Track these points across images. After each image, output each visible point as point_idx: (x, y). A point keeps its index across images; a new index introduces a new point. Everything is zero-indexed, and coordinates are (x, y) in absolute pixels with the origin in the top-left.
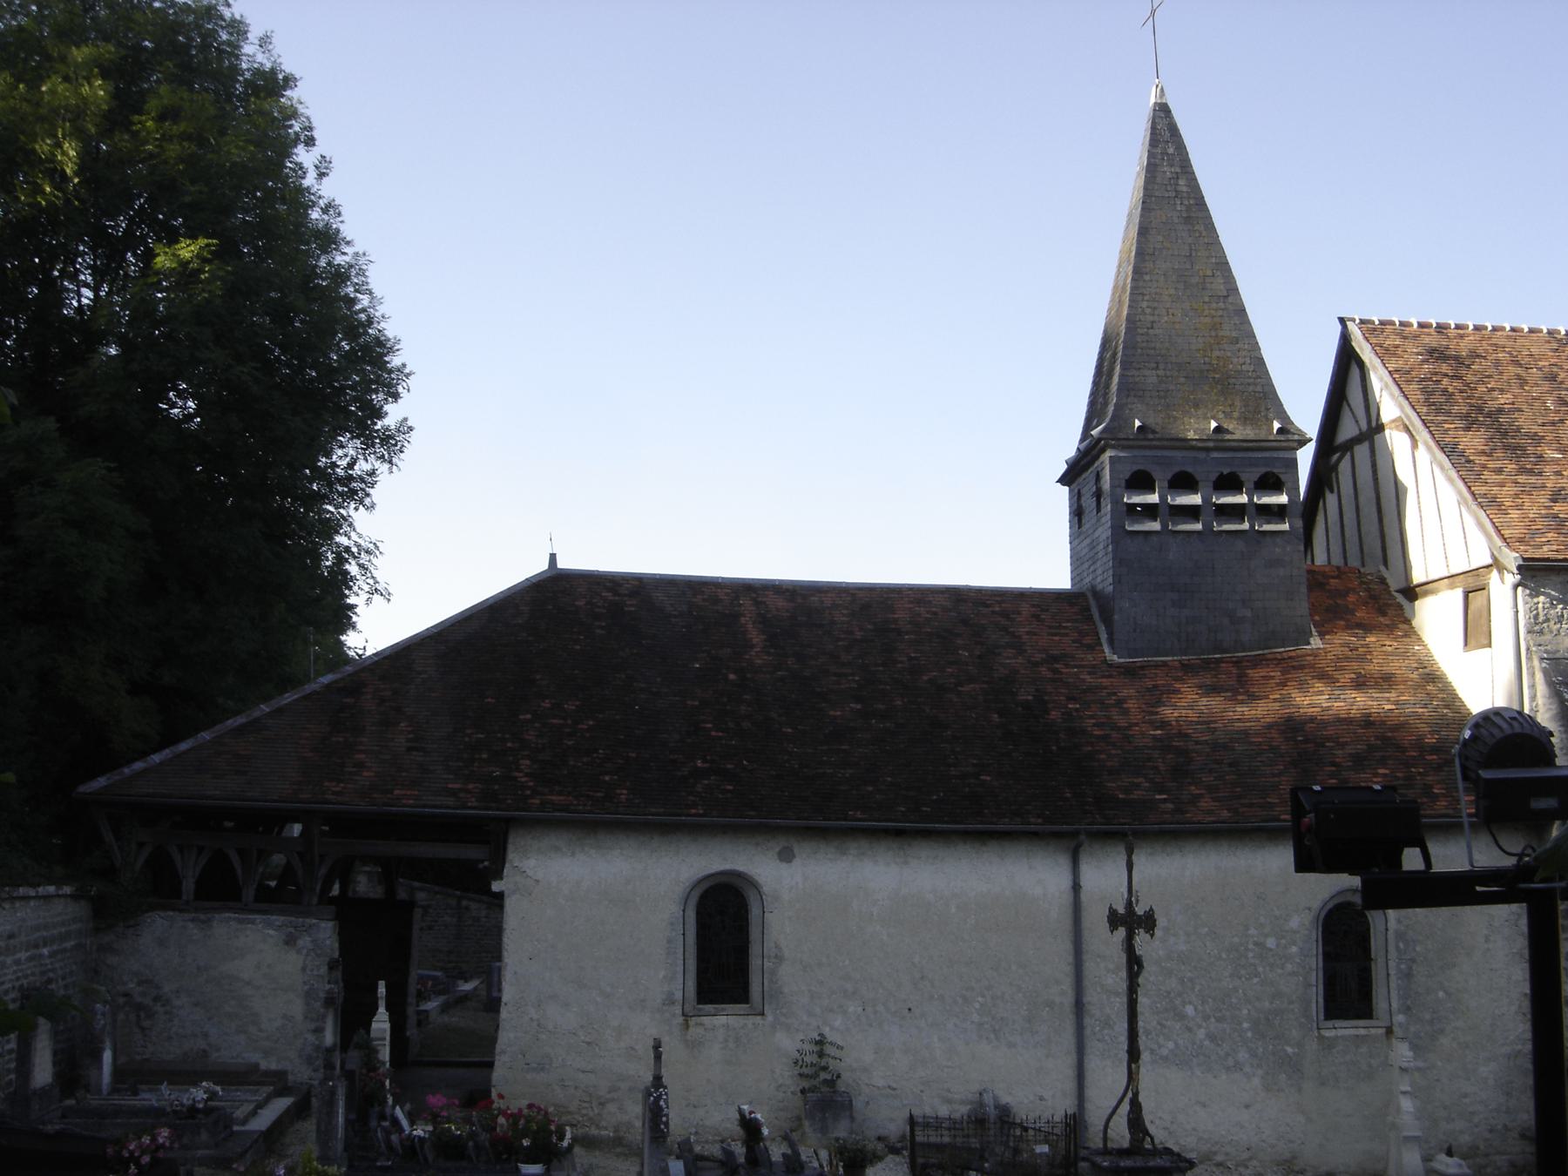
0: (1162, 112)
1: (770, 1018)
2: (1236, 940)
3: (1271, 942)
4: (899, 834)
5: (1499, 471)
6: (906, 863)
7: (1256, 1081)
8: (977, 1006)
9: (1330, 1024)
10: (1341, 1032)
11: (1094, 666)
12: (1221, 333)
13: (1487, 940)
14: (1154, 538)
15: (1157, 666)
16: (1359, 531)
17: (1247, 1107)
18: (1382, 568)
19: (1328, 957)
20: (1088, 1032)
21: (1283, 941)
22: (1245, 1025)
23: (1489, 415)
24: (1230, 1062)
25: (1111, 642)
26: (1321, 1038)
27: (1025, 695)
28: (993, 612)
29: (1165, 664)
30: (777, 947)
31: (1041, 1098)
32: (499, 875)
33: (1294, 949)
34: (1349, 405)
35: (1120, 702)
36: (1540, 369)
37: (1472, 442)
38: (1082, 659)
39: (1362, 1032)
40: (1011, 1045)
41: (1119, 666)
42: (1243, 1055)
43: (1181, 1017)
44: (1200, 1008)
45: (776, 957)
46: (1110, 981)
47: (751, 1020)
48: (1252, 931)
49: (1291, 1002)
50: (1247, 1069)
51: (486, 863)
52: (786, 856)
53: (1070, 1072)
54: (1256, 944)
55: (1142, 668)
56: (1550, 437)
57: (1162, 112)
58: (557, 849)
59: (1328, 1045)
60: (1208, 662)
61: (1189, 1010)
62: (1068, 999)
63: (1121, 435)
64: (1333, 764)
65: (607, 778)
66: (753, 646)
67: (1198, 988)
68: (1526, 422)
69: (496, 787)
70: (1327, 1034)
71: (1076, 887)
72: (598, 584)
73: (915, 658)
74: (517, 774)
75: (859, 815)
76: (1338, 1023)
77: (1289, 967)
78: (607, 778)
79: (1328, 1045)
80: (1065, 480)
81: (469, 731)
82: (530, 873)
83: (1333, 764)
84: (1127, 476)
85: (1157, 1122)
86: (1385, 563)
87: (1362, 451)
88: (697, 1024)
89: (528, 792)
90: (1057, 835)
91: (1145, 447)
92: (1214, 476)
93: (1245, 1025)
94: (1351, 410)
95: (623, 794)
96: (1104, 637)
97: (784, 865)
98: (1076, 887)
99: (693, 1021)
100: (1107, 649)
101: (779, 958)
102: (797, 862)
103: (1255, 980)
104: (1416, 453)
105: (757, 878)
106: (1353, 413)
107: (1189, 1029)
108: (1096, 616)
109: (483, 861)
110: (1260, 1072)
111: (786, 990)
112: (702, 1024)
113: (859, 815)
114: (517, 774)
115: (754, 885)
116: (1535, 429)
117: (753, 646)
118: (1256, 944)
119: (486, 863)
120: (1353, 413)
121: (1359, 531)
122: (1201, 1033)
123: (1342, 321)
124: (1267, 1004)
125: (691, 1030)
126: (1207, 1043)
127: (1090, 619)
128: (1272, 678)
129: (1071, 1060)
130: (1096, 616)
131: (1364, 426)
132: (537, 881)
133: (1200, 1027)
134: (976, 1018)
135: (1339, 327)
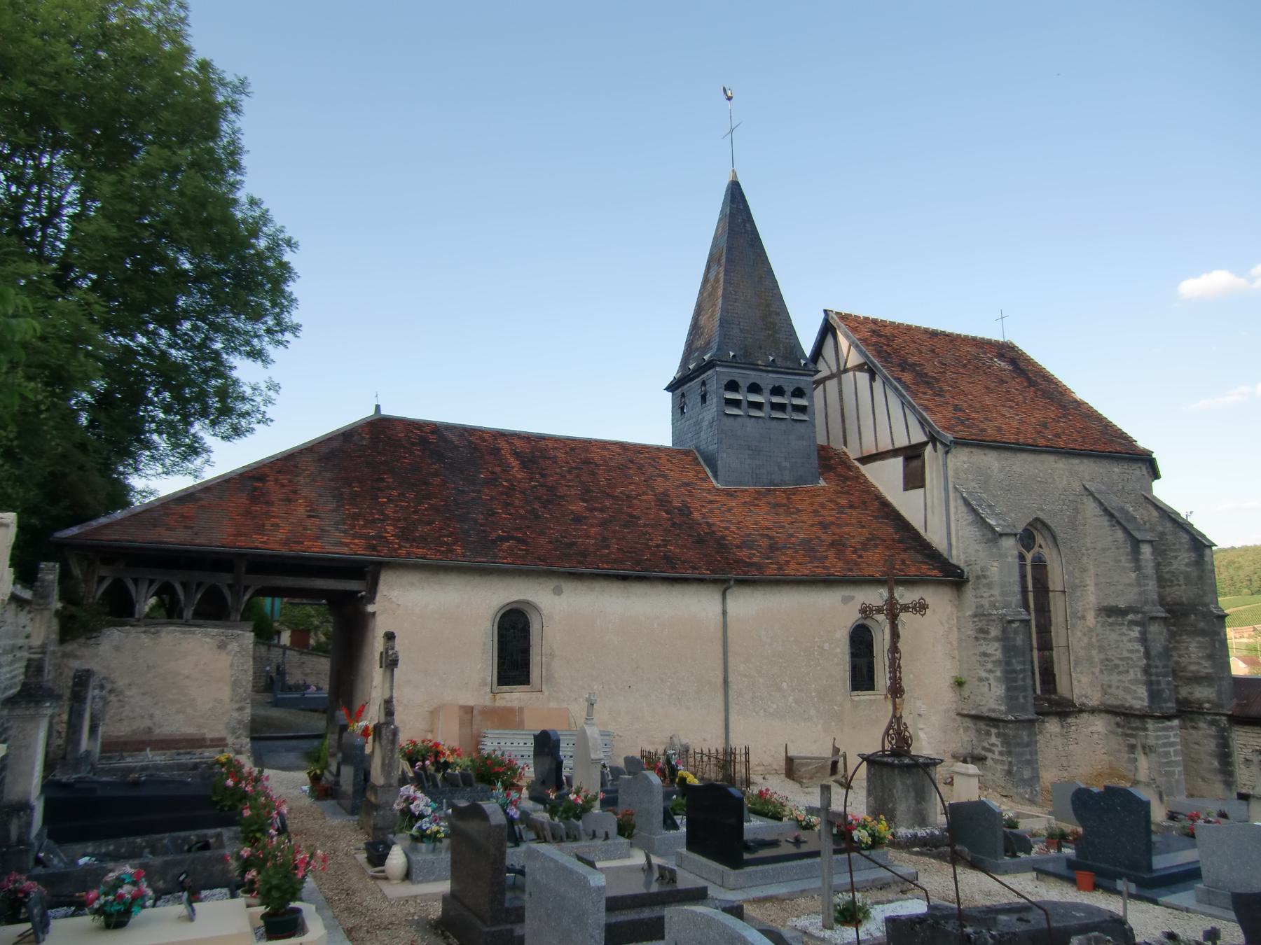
0: (735, 196)
1: (546, 693)
2: (809, 644)
3: (826, 646)
4: (624, 578)
5: (925, 393)
6: (628, 597)
7: (820, 727)
8: (668, 684)
9: (855, 693)
10: (862, 698)
11: (709, 490)
12: (771, 309)
13: (933, 646)
14: (739, 419)
15: (743, 491)
16: (827, 427)
17: (815, 742)
18: (844, 447)
19: (853, 655)
20: (730, 699)
21: (833, 646)
22: (814, 694)
23: (910, 365)
24: (806, 716)
25: (716, 476)
26: (852, 701)
27: (677, 503)
28: (646, 457)
29: (746, 490)
30: (551, 648)
31: (705, 740)
32: (371, 599)
33: (838, 650)
34: (824, 359)
35: (730, 510)
36: (926, 346)
37: (907, 377)
38: (701, 486)
39: (872, 697)
40: (688, 708)
41: (723, 490)
42: (813, 712)
43: (780, 689)
44: (790, 684)
45: (551, 654)
46: (742, 669)
47: (535, 695)
48: (817, 639)
49: (838, 681)
50: (815, 720)
51: (363, 593)
52: (558, 591)
53: (721, 724)
54: (818, 647)
55: (735, 492)
56: (943, 379)
57: (735, 196)
58: (412, 584)
59: (856, 705)
60: (769, 490)
61: (784, 685)
62: (720, 680)
63: (724, 359)
64: (851, 547)
65: (445, 539)
66: (513, 467)
67: (788, 672)
68: (928, 369)
69: (375, 542)
70: (857, 698)
71: (724, 613)
72: (409, 425)
73: (609, 480)
74: (387, 535)
75: (605, 566)
76: (859, 693)
77: (836, 660)
78: (445, 539)
79: (856, 705)
80: (671, 388)
81: (347, 507)
82: (394, 599)
83: (851, 547)
84: (726, 382)
85: (768, 752)
86: (845, 444)
87: (832, 385)
88: (501, 698)
89: (396, 546)
90: (715, 582)
91: (738, 368)
92: (771, 387)
93: (814, 694)
94: (825, 361)
95: (458, 549)
96: (710, 474)
97: (557, 597)
98: (724, 613)
99: (498, 696)
100: (713, 481)
101: (552, 655)
102: (564, 596)
103: (819, 668)
104: (873, 384)
105: (540, 605)
106: (827, 363)
107: (784, 697)
108: (702, 463)
109: (360, 592)
110: (821, 721)
111: (556, 675)
112: (504, 698)
113: (605, 566)
114: (387, 535)
115: (535, 608)
116: (934, 375)
117: (513, 467)
118: (818, 647)
119: (363, 593)
120: (827, 363)
121: (827, 427)
122: (791, 699)
123: (826, 311)
124: (824, 682)
125: (497, 701)
126: (793, 705)
127: (699, 464)
128: (805, 500)
129: (722, 715)
130: (702, 463)
131: (834, 369)
132: (399, 605)
133: (790, 695)
134: (667, 691)
135: (823, 316)
